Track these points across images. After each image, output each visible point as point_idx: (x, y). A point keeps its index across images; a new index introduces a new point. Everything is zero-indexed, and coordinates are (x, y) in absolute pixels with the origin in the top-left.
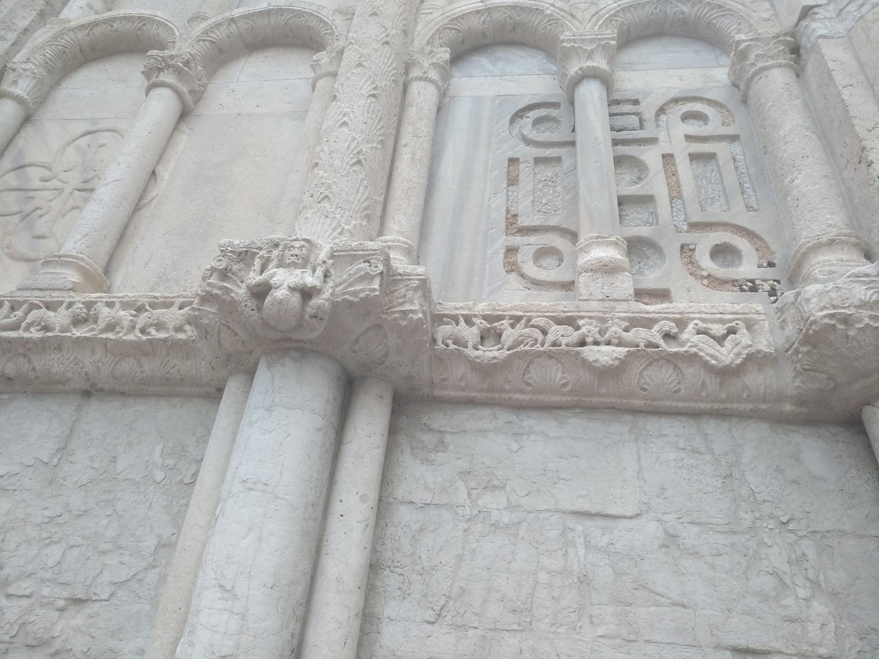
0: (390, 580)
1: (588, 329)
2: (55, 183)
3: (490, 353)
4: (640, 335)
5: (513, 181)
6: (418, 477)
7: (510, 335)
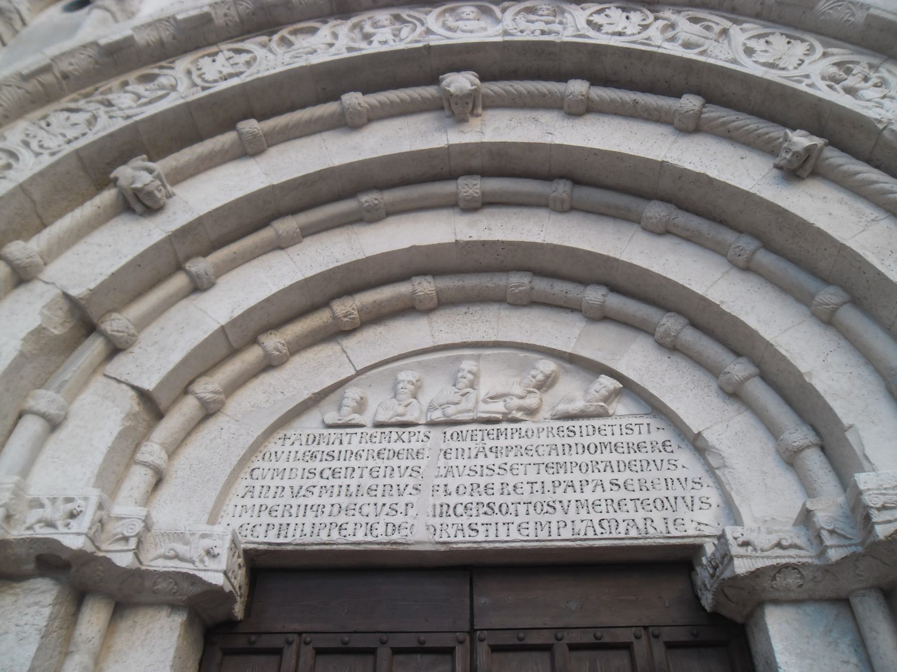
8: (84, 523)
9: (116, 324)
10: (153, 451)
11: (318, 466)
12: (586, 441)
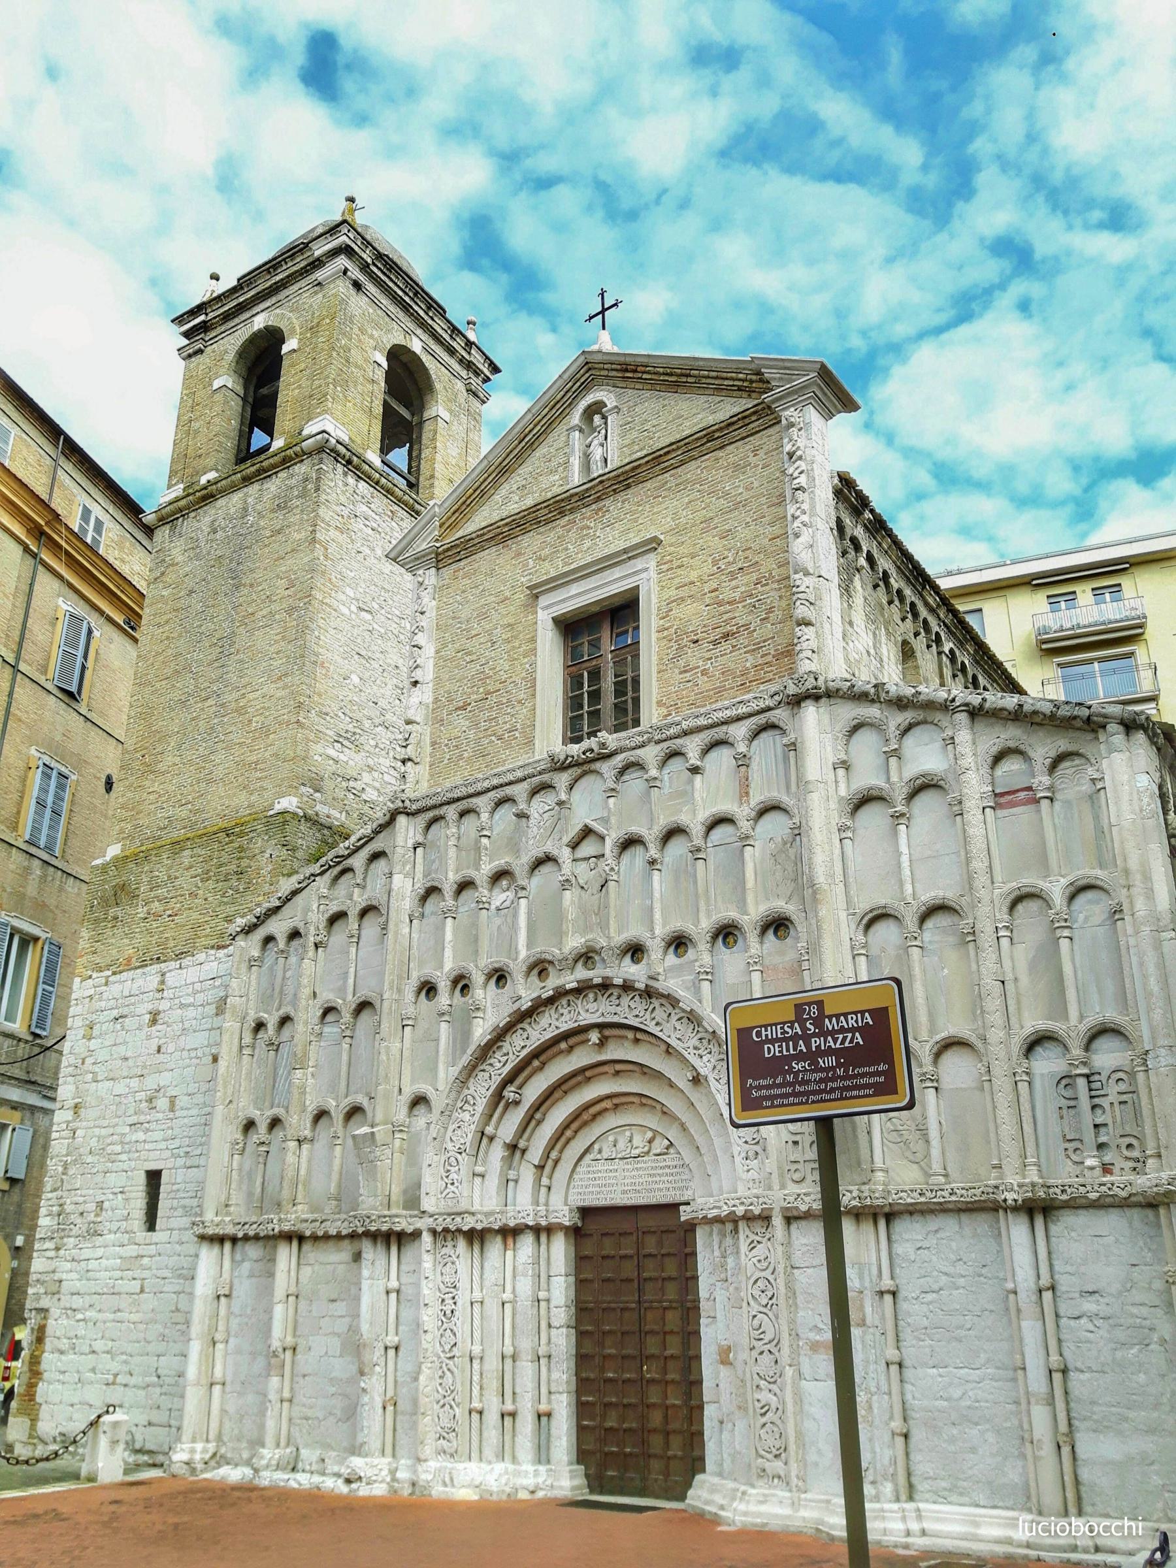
0: (1054, 1256)
1: (1089, 1188)
3: (1064, 1197)
5: (1062, 1118)
6: (1054, 1229)
7: (1069, 1191)
8: (531, 1218)
9: (522, 1144)
10: (545, 1181)
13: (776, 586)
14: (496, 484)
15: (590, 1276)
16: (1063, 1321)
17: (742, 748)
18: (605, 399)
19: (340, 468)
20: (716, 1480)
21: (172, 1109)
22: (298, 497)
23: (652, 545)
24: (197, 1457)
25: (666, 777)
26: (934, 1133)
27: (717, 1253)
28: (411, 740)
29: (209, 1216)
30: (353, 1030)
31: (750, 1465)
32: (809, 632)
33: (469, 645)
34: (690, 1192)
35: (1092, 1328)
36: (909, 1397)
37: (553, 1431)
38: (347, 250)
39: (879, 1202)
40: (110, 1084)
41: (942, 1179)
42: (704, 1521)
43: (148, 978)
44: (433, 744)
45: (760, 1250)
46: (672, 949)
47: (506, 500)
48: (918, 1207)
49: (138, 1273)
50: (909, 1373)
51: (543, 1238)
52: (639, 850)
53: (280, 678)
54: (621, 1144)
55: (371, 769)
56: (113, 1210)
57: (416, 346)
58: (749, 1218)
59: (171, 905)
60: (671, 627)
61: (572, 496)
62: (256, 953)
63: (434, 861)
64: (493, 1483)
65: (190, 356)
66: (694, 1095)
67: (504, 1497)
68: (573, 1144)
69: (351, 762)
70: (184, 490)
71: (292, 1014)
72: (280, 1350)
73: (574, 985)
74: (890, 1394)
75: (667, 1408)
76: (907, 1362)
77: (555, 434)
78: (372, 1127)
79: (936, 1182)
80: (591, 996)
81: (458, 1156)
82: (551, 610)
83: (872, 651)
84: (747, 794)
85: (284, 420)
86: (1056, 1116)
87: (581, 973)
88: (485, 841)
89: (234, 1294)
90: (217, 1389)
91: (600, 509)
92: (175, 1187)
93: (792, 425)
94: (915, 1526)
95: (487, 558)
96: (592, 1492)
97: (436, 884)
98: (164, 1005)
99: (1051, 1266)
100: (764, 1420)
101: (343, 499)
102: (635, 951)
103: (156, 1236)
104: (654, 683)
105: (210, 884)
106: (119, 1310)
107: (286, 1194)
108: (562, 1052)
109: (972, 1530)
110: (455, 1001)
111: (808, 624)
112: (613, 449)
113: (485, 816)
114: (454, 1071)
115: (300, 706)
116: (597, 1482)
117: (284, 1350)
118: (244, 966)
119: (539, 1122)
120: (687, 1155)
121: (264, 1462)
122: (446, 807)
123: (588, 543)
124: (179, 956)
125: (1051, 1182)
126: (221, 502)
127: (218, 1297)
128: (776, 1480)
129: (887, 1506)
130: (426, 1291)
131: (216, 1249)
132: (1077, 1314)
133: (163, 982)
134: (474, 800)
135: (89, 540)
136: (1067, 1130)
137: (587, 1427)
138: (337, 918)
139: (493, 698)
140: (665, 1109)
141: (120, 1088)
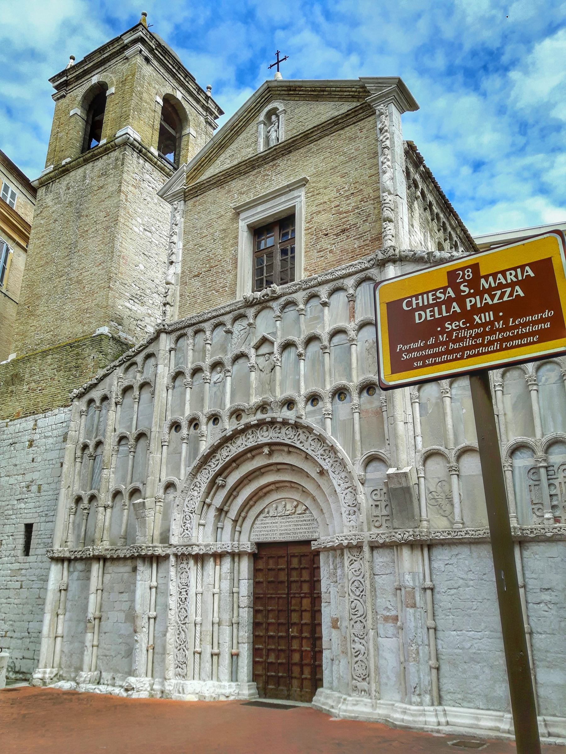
0: (525, 568)
1: (547, 530)
2: (439, 497)
3: (532, 535)
4: (555, 530)
5: (531, 491)
6: (526, 553)
7: (535, 532)
8: (230, 548)
9: (226, 508)
10: (238, 528)
11: (263, 526)
12: (301, 519)
13: (372, 202)
14: (217, 155)
15: (261, 580)
16: (530, 605)
17: (351, 291)
18: (278, 107)
19: (135, 154)
20: (329, 692)
21: (39, 492)
22: (112, 169)
23: (303, 182)
24: (47, 676)
25: (309, 309)
26: (456, 500)
27: (331, 567)
28: (169, 293)
29: (56, 547)
30: (135, 448)
31: (348, 684)
32: (390, 226)
33: (201, 241)
34: (317, 534)
35: (547, 609)
36: (440, 647)
37: (240, 664)
38: (141, 40)
39: (425, 538)
40: (7, 478)
41: (461, 526)
42: (322, 715)
43: (28, 423)
44: (181, 295)
45: (356, 565)
46: (309, 402)
47: (223, 163)
48: (447, 541)
49: (19, 578)
50: (440, 634)
51: (236, 559)
52: (293, 349)
53: (100, 264)
54: (280, 508)
55: (150, 316)
56: (7, 545)
57: (179, 96)
58: (350, 547)
59: (41, 384)
60: (312, 227)
61: (259, 158)
62: (84, 408)
63: (180, 358)
64: (206, 692)
65: (58, 99)
66: (321, 481)
67: (212, 700)
68: (253, 508)
69: (138, 311)
70: (53, 168)
71: (103, 440)
72: (92, 619)
73: (256, 422)
74: (429, 645)
75: (302, 651)
76: (439, 628)
77: (250, 126)
78: (144, 499)
79: (457, 527)
80: (265, 428)
81: (191, 515)
82: (246, 221)
83: (423, 243)
84: (354, 316)
85: (107, 131)
86: (527, 490)
87: (260, 416)
88: (208, 346)
89: (69, 589)
90: (59, 639)
91: (274, 165)
92: (40, 533)
93: (382, 114)
94: (443, 720)
95: (212, 194)
96: (260, 697)
97: (181, 370)
98: (36, 437)
99: (524, 574)
100: (357, 659)
101: (136, 170)
102: (290, 403)
103: (30, 558)
104: (303, 258)
105: (62, 373)
106: (9, 598)
107: (97, 535)
108: (248, 459)
109: (476, 722)
110: (191, 433)
111: (391, 221)
112: (281, 133)
113: (208, 333)
114: (190, 469)
115: (110, 278)
116: (263, 691)
117: (95, 619)
118: (77, 415)
119: (235, 497)
120: (315, 513)
121: (82, 679)
122: (187, 329)
123: (267, 184)
124: (44, 411)
125: (525, 527)
126: (72, 174)
127: (60, 590)
128: (363, 693)
129: (427, 708)
130: (171, 587)
131: (60, 566)
132: (539, 601)
133: (36, 425)
134: (203, 325)
135: (8, 202)
136: (534, 498)
137: (258, 662)
138: (127, 389)
139: (214, 270)
140: (304, 489)
141: (12, 480)
